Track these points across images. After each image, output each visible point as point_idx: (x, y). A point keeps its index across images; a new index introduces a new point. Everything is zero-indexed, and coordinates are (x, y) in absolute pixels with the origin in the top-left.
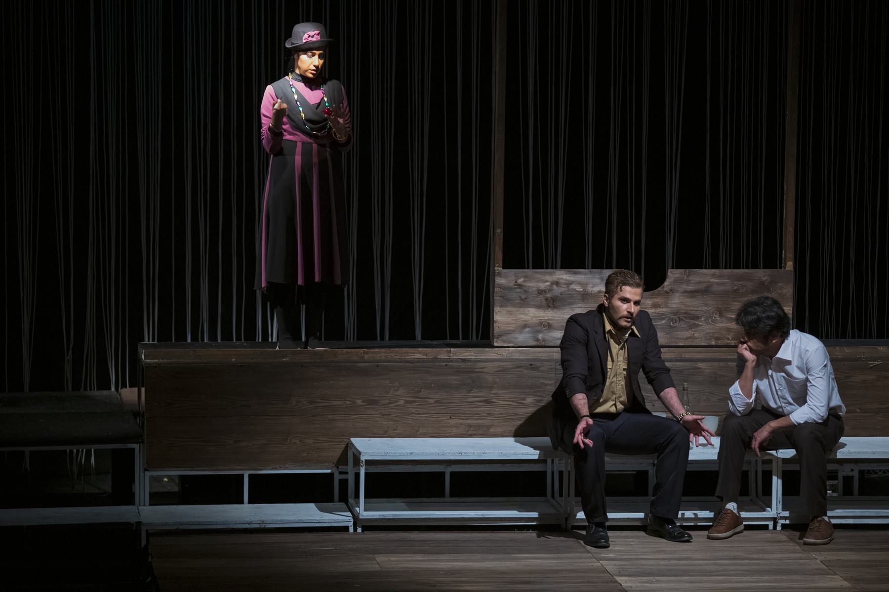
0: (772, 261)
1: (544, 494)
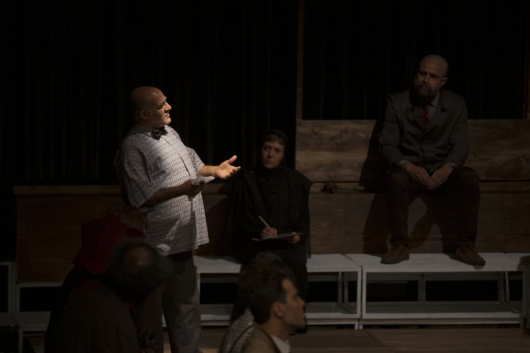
1: (336, 300)
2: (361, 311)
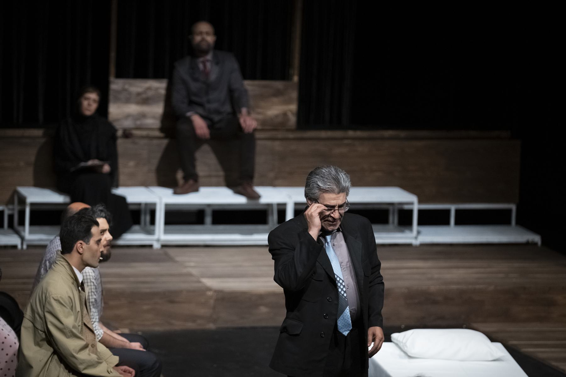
0: (285, 76)
2: (159, 232)
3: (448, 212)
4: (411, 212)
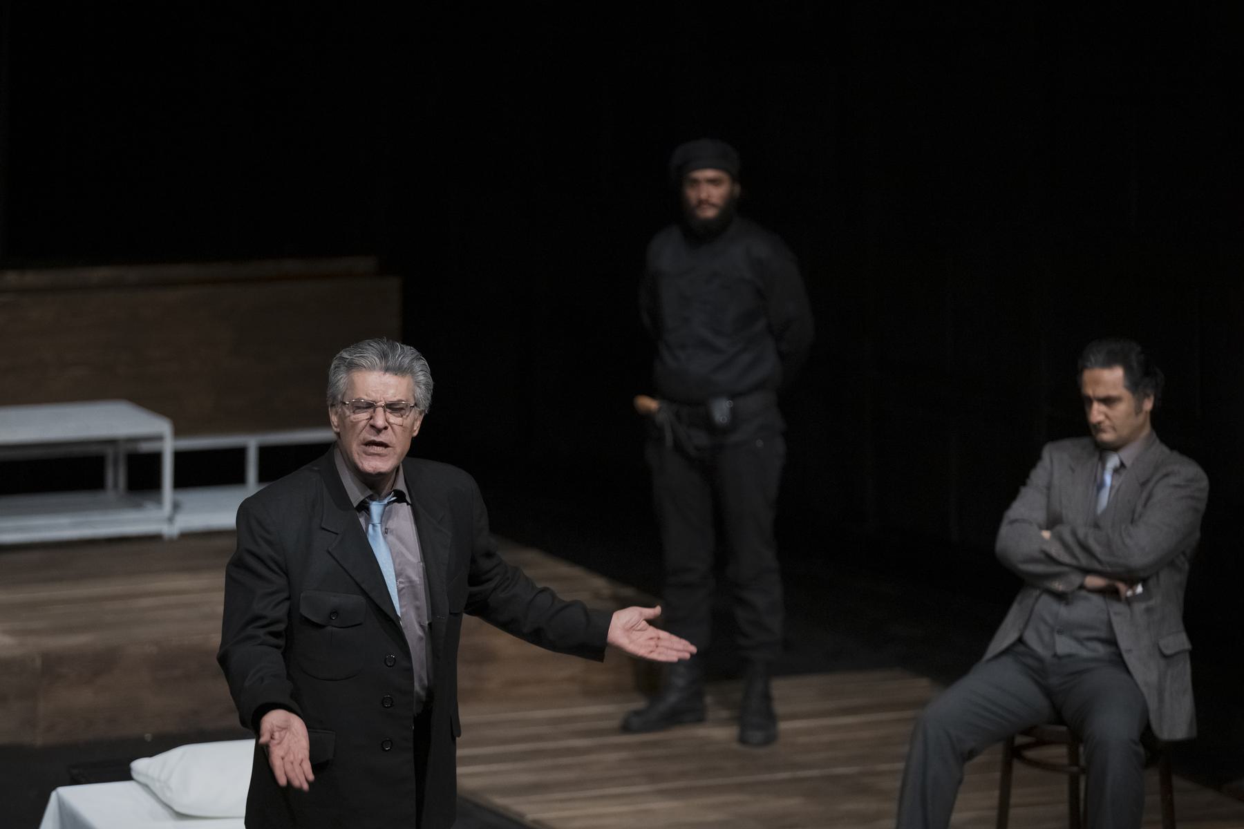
3: (240, 452)
4: (156, 458)
